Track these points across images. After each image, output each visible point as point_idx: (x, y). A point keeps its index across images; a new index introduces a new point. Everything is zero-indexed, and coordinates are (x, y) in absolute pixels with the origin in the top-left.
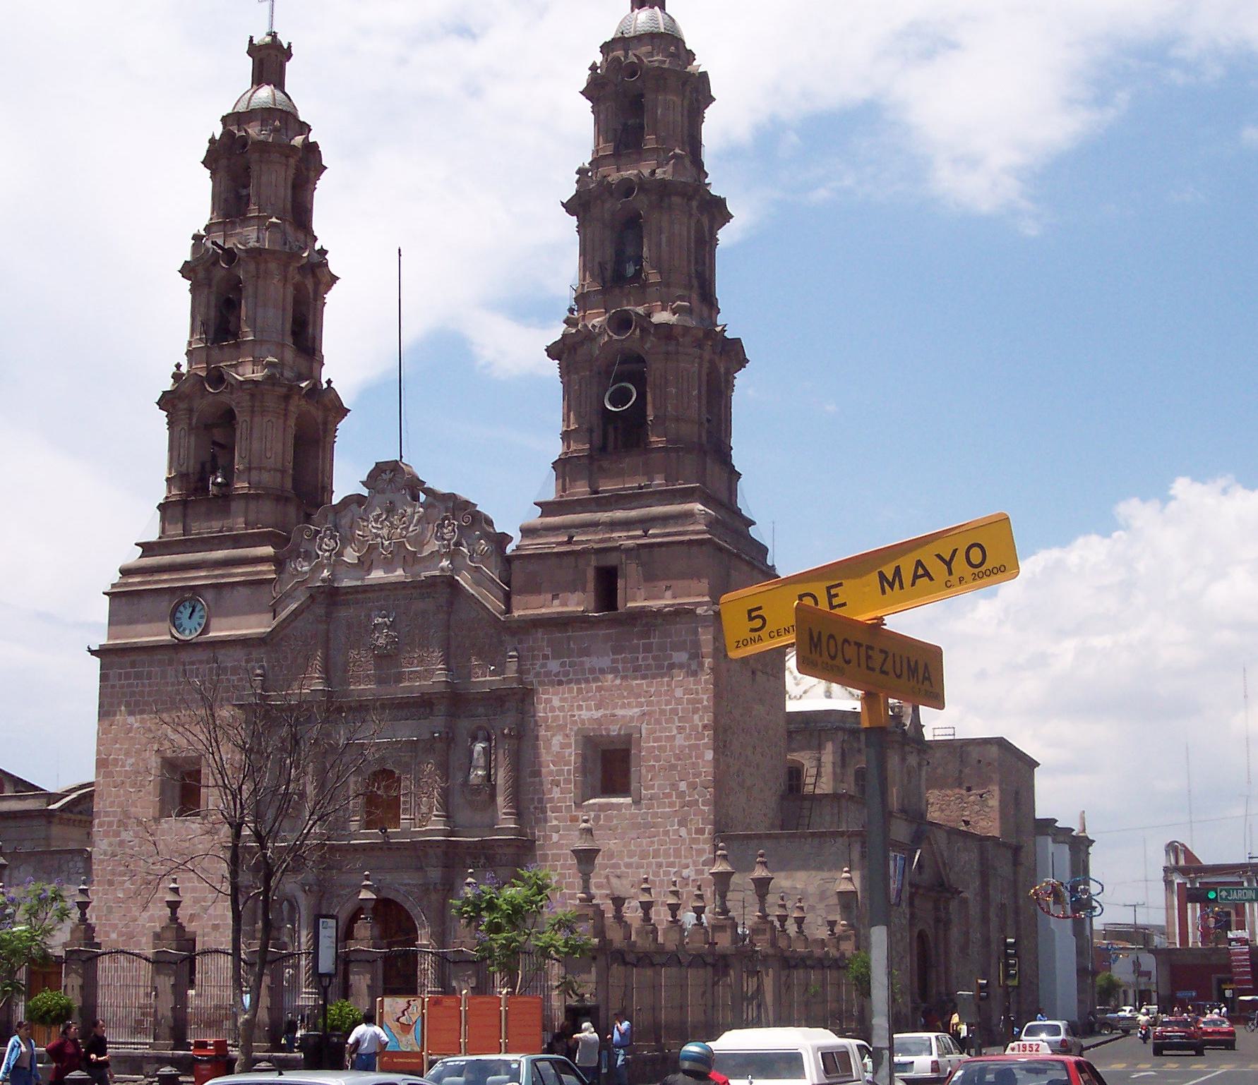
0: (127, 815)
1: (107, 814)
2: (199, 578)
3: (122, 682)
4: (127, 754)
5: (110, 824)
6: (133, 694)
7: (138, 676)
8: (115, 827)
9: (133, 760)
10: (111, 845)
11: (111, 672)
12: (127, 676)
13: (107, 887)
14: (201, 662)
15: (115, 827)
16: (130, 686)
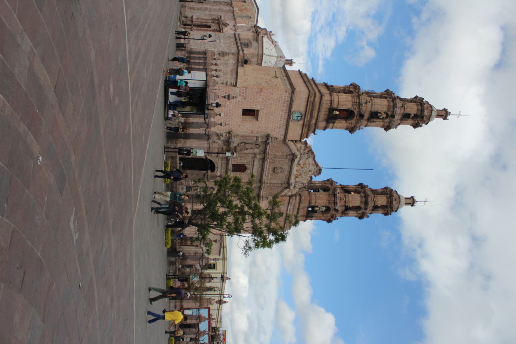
0: (245, 98)
1: (246, 92)
2: (308, 118)
3: (283, 97)
4: (263, 99)
5: (243, 93)
6: (279, 101)
7: (284, 102)
8: (242, 94)
9: (260, 100)
10: (237, 93)
11: (287, 94)
12: (285, 99)
13: (225, 91)
14: (284, 122)
15: (242, 94)
16: (282, 100)
